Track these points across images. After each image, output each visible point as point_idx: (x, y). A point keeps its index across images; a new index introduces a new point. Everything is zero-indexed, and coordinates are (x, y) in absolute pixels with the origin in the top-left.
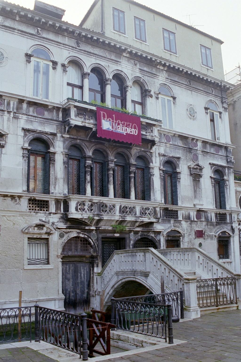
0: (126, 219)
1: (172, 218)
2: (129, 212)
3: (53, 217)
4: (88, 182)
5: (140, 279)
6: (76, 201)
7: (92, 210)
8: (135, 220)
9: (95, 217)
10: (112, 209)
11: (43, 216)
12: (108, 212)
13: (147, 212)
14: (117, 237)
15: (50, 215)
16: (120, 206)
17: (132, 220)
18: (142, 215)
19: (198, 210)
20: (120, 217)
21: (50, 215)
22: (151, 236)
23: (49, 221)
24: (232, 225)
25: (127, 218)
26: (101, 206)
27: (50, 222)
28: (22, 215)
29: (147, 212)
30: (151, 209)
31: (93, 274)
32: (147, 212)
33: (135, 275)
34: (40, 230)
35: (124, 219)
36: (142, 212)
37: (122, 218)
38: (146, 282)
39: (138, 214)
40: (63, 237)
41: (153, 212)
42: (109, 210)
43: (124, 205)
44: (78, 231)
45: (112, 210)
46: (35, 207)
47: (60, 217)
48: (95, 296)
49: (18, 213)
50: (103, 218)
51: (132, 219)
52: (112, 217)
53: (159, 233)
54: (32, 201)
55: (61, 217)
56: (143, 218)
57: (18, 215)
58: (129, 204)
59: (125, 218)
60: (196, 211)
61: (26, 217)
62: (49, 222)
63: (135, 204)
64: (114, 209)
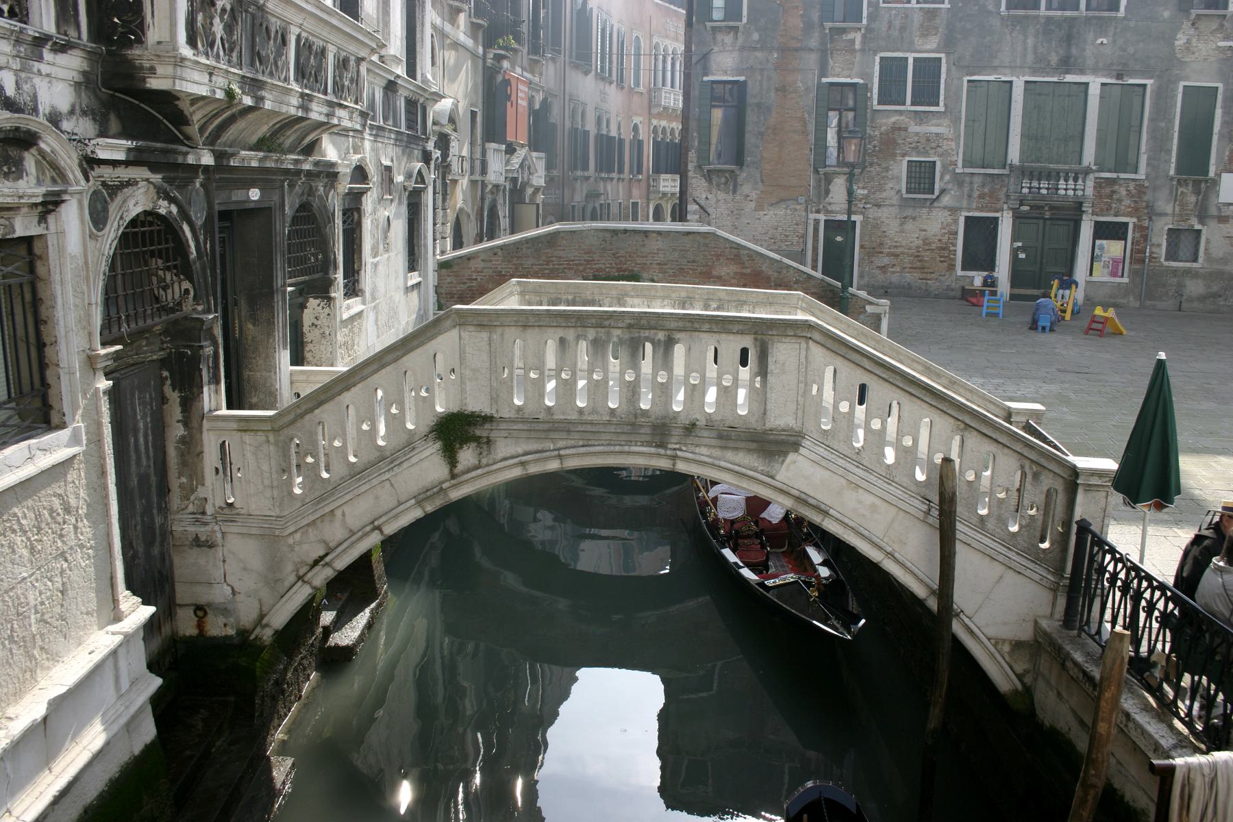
5: (723, 464)
16: (299, 37)
19: (390, 81)
21: (40, 58)
23: (35, 98)
24: (424, 148)
27: (41, 108)
31: (186, 423)
33: (662, 445)
38: (772, 477)
47: (78, 78)
48: (220, 541)
55: (84, 73)
60: (383, 83)
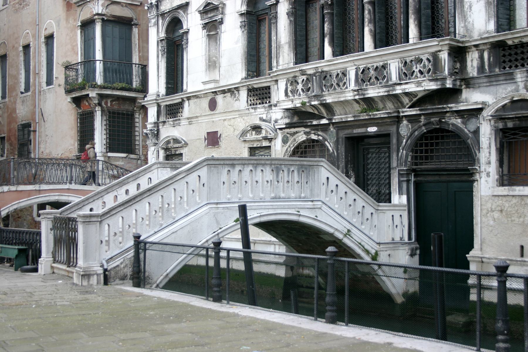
0: (368, 94)
1: (516, 66)
2: (373, 77)
3: (276, 111)
4: (327, 33)
6: (285, 80)
7: (308, 90)
8: (386, 94)
9: (312, 101)
10: (341, 80)
11: (263, 113)
12: (335, 86)
13: (416, 68)
14: (372, 133)
15: (272, 109)
16: (357, 69)
17: (379, 94)
18: (403, 80)
20: (356, 93)
21: (272, 109)
22: (453, 125)
25: (369, 92)
26: (323, 77)
28: (241, 116)
29: (416, 68)
30: (424, 59)
32: (416, 68)
34: (258, 135)
35: (364, 95)
36: (404, 71)
37: (358, 95)
39: (394, 78)
40: (287, 142)
41: (430, 67)
42: (336, 82)
43: (365, 66)
44: (308, 130)
45: (342, 81)
46: (257, 100)
49: (237, 113)
50: (325, 100)
51: (379, 92)
52: (340, 96)
53: (476, 112)
54: (252, 91)
56: (404, 87)
57: (237, 116)
58: (371, 61)
59: (366, 92)
61: (246, 118)
62: (271, 120)
63: (385, 58)
64: (345, 79)
